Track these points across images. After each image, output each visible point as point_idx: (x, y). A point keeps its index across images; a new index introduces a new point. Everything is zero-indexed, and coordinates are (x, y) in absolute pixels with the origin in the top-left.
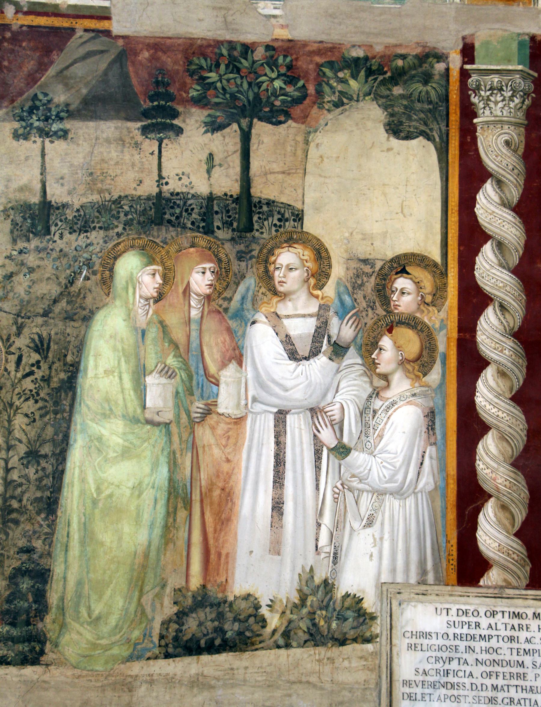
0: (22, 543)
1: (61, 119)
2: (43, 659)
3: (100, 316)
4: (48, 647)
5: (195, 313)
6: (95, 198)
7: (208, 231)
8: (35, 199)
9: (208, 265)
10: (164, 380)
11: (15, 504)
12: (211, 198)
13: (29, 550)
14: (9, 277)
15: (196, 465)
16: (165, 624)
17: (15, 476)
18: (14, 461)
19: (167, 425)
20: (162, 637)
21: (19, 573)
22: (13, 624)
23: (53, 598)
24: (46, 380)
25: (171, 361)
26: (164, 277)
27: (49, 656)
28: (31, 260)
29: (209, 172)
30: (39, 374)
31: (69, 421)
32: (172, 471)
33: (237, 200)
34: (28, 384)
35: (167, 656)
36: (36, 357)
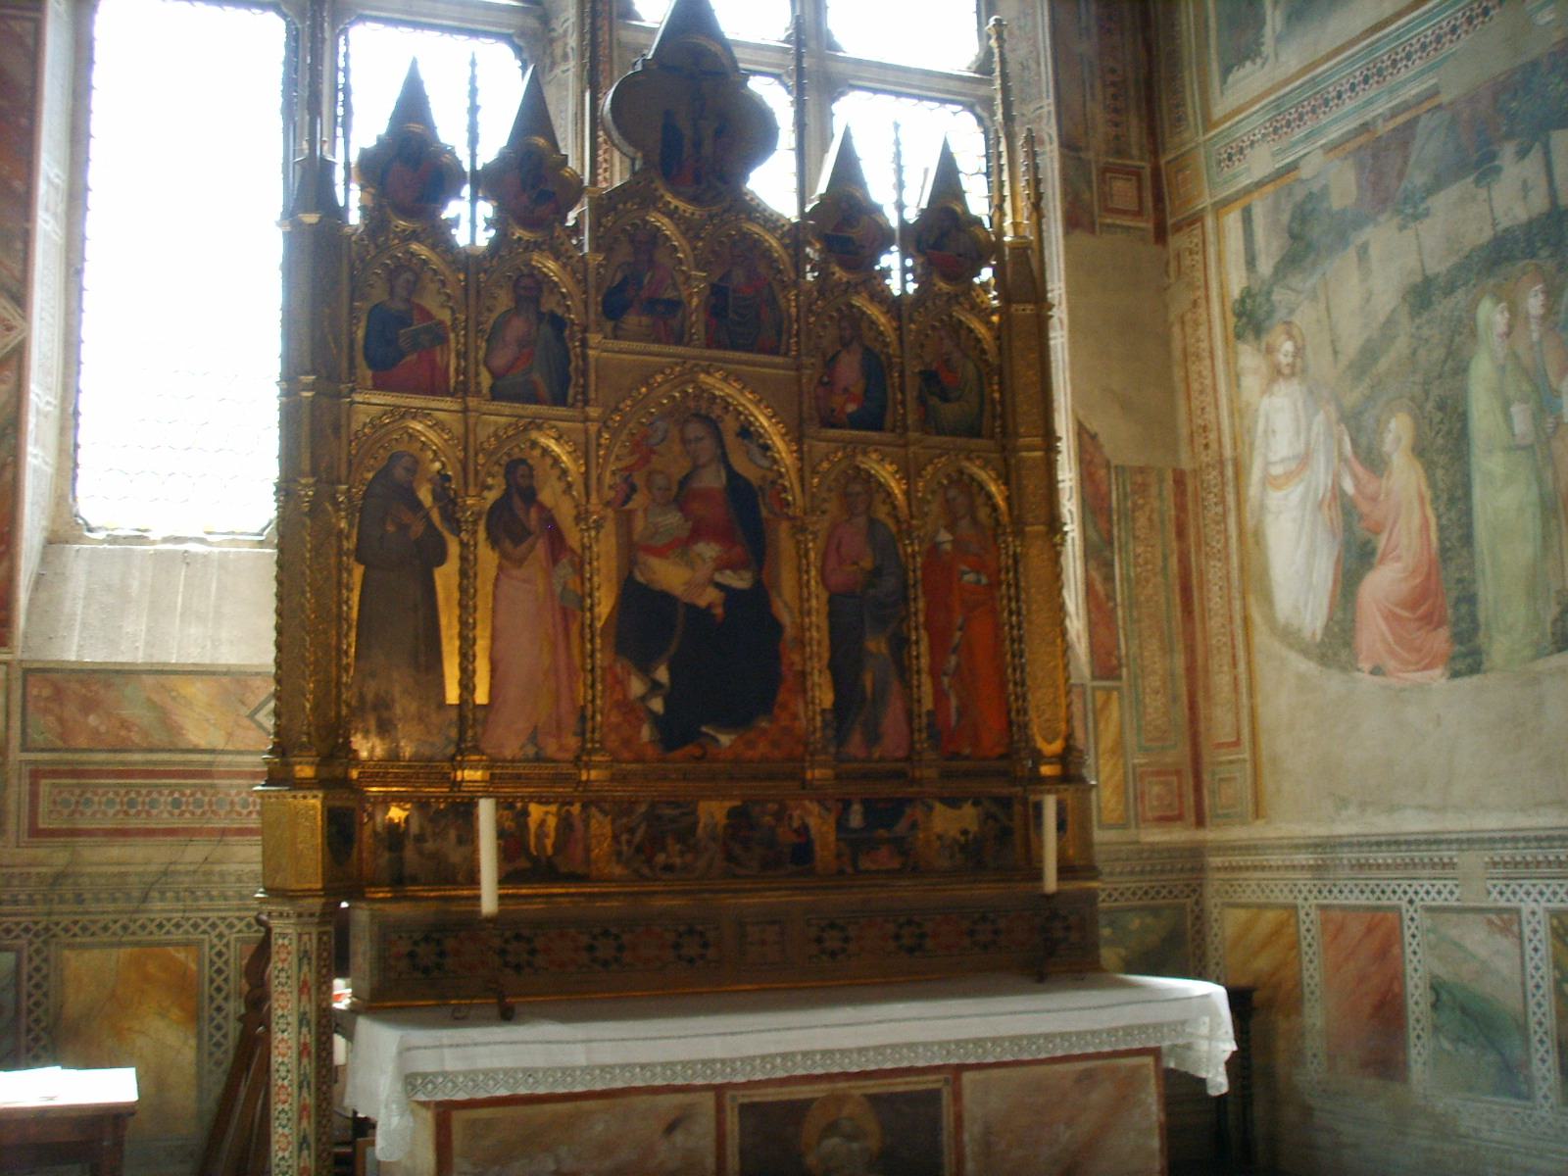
0: (1457, 576)
1: (1423, 199)
2: (1483, 667)
3: (1473, 365)
4: (1484, 657)
5: (1535, 336)
6: (1454, 259)
7: (1533, 255)
8: (1418, 279)
9: (1539, 287)
10: (1524, 406)
11: (1448, 544)
12: (1530, 222)
13: (1460, 581)
14: (1414, 352)
15: (1556, 479)
16: (1555, 622)
17: (1444, 521)
18: (1442, 509)
19: (1532, 446)
20: (1553, 634)
21: (1458, 601)
22: (1461, 643)
23: (1481, 617)
24: (1449, 432)
25: (1526, 387)
26: (1510, 311)
27: (1486, 665)
28: (1426, 332)
29: (1525, 197)
30: (1445, 428)
31: (1468, 463)
32: (1540, 487)
33: (1549, 215)
34: (1440, 441)
35: (1560, 650)
36: (1440, 415)
